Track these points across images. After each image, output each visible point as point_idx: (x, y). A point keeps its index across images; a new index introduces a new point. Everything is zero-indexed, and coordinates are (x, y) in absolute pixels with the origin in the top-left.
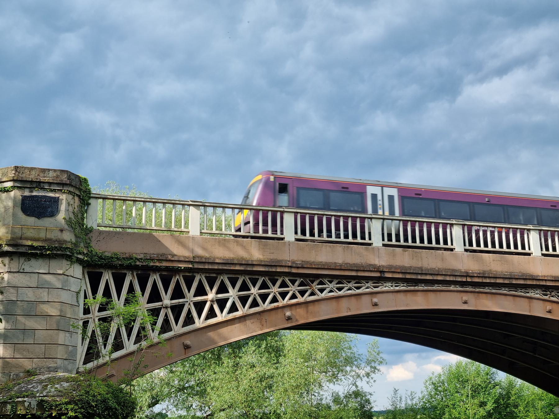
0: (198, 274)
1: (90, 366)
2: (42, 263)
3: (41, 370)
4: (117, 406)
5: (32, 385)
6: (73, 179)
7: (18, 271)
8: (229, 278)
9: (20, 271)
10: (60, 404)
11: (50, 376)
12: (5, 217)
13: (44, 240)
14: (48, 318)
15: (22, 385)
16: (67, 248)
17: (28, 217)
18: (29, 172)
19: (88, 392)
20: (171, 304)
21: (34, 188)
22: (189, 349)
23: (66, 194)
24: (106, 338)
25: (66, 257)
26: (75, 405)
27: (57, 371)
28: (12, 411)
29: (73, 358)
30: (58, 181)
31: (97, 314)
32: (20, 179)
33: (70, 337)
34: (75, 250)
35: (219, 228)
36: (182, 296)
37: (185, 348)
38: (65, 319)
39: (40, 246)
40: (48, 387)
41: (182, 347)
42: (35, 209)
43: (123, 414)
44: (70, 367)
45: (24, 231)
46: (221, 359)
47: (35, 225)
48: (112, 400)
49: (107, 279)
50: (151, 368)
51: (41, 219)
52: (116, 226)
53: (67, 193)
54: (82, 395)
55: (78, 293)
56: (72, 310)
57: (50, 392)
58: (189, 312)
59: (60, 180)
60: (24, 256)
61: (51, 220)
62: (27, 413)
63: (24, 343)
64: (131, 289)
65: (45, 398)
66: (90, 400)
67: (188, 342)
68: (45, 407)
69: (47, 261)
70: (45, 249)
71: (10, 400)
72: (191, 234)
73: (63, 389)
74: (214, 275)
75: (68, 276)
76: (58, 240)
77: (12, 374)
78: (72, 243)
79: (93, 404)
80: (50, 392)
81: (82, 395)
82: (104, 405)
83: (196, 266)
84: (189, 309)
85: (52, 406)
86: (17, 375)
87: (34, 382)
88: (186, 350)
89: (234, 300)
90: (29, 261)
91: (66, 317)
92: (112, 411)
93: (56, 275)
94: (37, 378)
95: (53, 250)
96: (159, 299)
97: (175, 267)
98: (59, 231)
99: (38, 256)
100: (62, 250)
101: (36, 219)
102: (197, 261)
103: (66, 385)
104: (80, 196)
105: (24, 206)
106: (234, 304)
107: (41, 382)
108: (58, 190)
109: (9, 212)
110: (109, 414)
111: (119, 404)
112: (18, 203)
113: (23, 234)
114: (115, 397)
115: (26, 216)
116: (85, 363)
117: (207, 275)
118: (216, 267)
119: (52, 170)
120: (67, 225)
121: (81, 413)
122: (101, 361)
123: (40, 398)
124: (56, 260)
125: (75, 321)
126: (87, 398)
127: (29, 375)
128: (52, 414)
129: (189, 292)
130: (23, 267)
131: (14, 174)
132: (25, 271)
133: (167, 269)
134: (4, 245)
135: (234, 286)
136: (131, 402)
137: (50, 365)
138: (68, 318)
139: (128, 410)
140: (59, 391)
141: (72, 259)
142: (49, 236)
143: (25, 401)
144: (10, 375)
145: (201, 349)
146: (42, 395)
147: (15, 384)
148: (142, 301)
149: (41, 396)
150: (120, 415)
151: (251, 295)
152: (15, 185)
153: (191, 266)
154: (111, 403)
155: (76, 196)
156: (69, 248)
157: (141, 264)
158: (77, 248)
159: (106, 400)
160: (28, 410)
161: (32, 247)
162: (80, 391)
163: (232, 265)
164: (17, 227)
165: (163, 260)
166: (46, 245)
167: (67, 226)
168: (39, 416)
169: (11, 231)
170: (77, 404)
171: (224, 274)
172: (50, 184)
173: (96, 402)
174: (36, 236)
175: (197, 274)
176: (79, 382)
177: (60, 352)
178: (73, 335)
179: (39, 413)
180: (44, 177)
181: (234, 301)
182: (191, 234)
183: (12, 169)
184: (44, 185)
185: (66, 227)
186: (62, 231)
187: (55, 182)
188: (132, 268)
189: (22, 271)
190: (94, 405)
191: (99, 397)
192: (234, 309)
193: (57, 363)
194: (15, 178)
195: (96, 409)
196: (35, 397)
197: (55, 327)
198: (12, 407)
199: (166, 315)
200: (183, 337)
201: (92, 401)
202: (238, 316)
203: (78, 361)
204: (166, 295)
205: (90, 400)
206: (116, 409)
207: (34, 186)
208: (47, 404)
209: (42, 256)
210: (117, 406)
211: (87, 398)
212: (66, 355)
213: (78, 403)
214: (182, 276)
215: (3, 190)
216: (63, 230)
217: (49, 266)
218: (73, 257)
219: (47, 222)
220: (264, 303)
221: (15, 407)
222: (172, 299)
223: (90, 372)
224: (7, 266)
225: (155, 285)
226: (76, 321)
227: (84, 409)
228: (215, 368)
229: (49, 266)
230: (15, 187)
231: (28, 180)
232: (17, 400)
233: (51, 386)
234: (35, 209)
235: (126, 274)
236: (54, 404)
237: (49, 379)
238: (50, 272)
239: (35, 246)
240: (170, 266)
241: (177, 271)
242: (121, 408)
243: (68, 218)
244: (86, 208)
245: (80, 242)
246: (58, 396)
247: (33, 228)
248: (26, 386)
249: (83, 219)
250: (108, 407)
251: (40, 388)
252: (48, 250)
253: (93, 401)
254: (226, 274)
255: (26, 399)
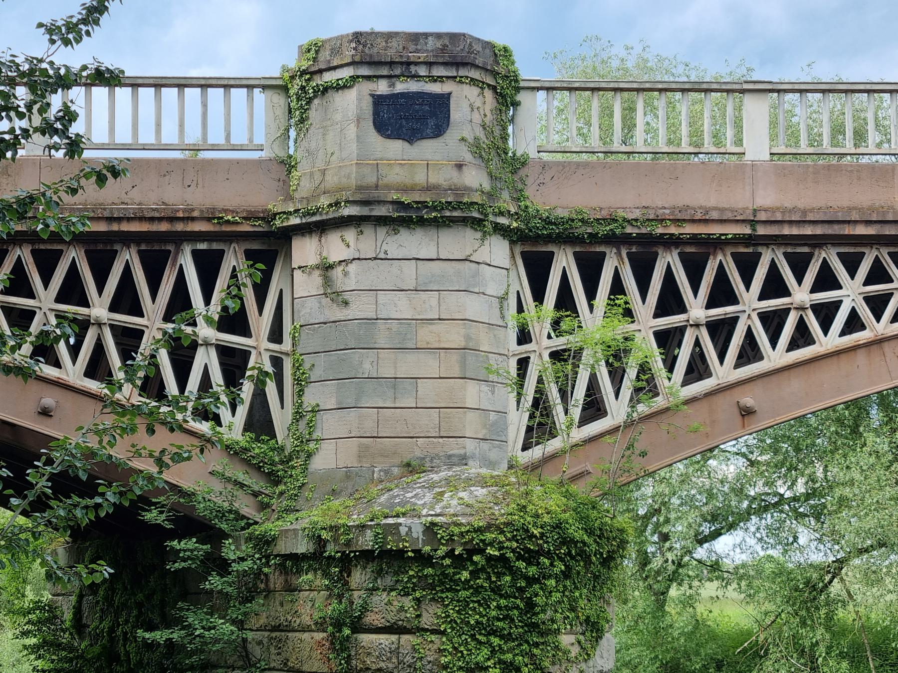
0: (768, 247)
1: (537, 452)
2: (423, 237)
3: (435, 461)
4: (585, 537)
5: (414, 493)
6: (478, 52)
7: (374, 256)
8: (839, 255)
9: (379, 256)
10: (468, 531)
11: (450, 473)
12: (343, 144)
13: (423, 188)
14: (442, 355)
15: (396, 492)
16: (473, 203)
17: (388, 140)
18: (384, 44)
19: (524, 507)
20: (706, 317)
21: (398, 77)
22: (752, 417)
23: (465, 85)
24: (565, 395)
25: (473, 224)
26: (498, 534)
27: (466, 464)
28: (377, 544)
29: (499, 436)
30: (447, 59)
31: (546, 342)
32: (368, 60)
33: (490, 393)
34: (491, 207)
35: (815, 140)
36: (732, 299)
37: (743, 413)
38: (477, 356)
39: (417, 202)
40: (445, 496)
41: (736, 411)
42: (401, 124)
43: (601, 554)
44: (493, 455)
45: (383, 171)
46: (861, 435)
47: (405, 157)
48: (574, 525)
49: (564, 267)
50: (668, 458)
51: (416, 144)
52: (578, 150)
53: (467, 83)
54: (511, 514)
55: (503, 299)
56: (492, 335)
57: (448, 506)
58: (750, 335)
59: (450, 57)
60: (385, 225)
61: (437, 144)
62: (406, 547)
63: (397, 405)
64: (617, 287)
65: (438, 520)
66: (530, 524)
67: (748, 401)
68: (439, 536)
69: (432, 232)
70: (427, 207)
71: (372, 520)
72: (748, 157)
73: (474, 502)
74: (806, 250)
75: (478, 263)
76: (453, 187)
77: (376, 469)
78: (483, 192)
79: (535, 532)
80: (448, 506)
81: (511, 514)
82: (559, 533)
83: (761, 231)
84: (749, 328)
85: (453, 535)
86: (386, 472)
87: (418, 485)
88: (746, 418)
89: (853, 304)
90: (396, 234)
91: (479, 351)
92: (576, 546)
93: (453, 262)
94: (424, 478)
95: (443, 209)
96: (680, 307)
97: (712, 234)
98: (455, 168)
99: (414, 223)
100: (462, 209)
101: (406, 144)
102: (764, 219)
103: (480, 492)
104: (496, 87)
105: (378, 117)
106: (853, 314)
107: (431, 486)
108: (448, 77)
109: (350, 131)
110: (569, 554)
111: (590, 533)
112: (366, 112)
113: (380, 177)
114: (582, 518)
115: (385, 139)
116: (524, 449)
117: (789, 250)
118: (808, 231)
119: (431, 34)
120: (470, 153)
121: (513, 551)
122: (554, 445)
123: (429, 519)
124: (451, 230)
125: (500, 358)
126: (522, 520)
127: (411, 472)
128: (453, 550)
129: (748, 287)
130: (385, 247)
131: (355, 49)
132: (388, 257)
133: (695, 239)
134: (343, 203)
135: (852, 274)
136: (618, 530)
137: (451, 452)
138: (483, 353)
139: (612, 545)
140: (467, 506)
141: (484, 226)
142: (434, 179)
143: (400, 524)
144: (373, 472)
145: (779, 415)
146: (433, 513)
147: (382, 490)
148: (643, 313)
149: (432, 515)
150: (595, 555)
151: (894, 291)
152: (359, 73)
153: (747, 230)
154: (572, 531)
155: (487, 89)
156: (476, 203)
157: (637, 231)
158: (494, 201)
159: (561, 524)
160: (407, 542)
161: (398, 204)
162: (508, 505)
163: (846, 226)
164: (367, 164)
165: (684, 220)
166: (428, 200)
167: (471, 157)
168: (429, 554)
169: (356, 172)
170: (502, 532)
171: (829, 246)
172: (430, 64)
173: (542, 528)
174: (408, 181)
175: (765, 248)
176: (508, 488)
177: (471, 425)
178: (496, 388)
179: (427, 549)
180: (417, 51)
181: (853, 308)
182: (748, 157)
183: (351, 38)
184: (417, 68)
185: (468, 157)
186: (459, 166)
187: (441, 60)
188: (615, 240)
189: (383, 257)
190: (538, 535)
191: (546, 519)
192: (854, 323)
193: (465, 448)
194: (357, 59)
195: (541, 542)
196: (419, 517)
197: (456, 373)
198: (376, 536)
199: (697, 343)
200: (737, 391)
201: (533, 526)
202: (865, 341)
203: (510, 443)
204: (696, 298)
205: (530, 524)
206: (584, 543)
207: (398, 72)
208: (443, 531)
209: (422, 222)
210: (585, 537)
211: (522, 520)
212: (484, 431)
213: (505, 529)
214: (732, 254)
215: (334, 85)
216: (462, 165)
217: (438, 244)
218: (486, 223)
219: (428, 149)
220: (878, 319)
221: (380, 536)
222: (709, 306)
223: (534, 467)
224: (352, 248)
225: (669, 277)
226: (501, 360)
227: (517, 541)
228: (845, 456)
229: (438, 244)
230: (358, 77)
231: (383, 60)
232: (384, 521)
233: (450, 494)
234: (401, 124)
235: (604, 255)
236: (456, 530)
237: (447, 480)
238: (441, 257)
239: (406, 203)
240: (701, 234)
241: (716, 244)
242: (595, 541)
243: (473, 138)
244: (511, 113)
245: (500, 189)
246: (464, 515)
247: (401, 164)
248: (402, 495)
249: (504, 138)
250: (565, 538)
251: (429, 497)
252: (434, 208)
253: (535, 525)
254: (833, 245)
255: (401, 520)
